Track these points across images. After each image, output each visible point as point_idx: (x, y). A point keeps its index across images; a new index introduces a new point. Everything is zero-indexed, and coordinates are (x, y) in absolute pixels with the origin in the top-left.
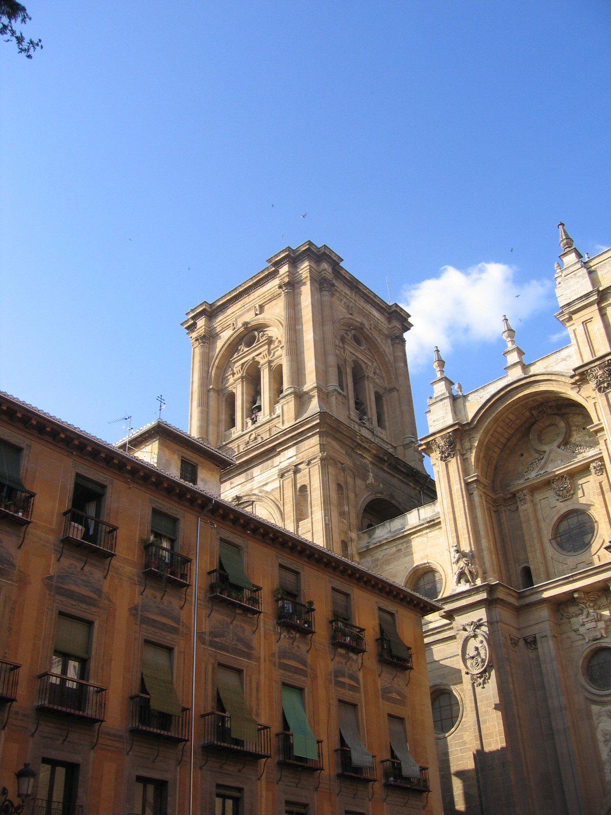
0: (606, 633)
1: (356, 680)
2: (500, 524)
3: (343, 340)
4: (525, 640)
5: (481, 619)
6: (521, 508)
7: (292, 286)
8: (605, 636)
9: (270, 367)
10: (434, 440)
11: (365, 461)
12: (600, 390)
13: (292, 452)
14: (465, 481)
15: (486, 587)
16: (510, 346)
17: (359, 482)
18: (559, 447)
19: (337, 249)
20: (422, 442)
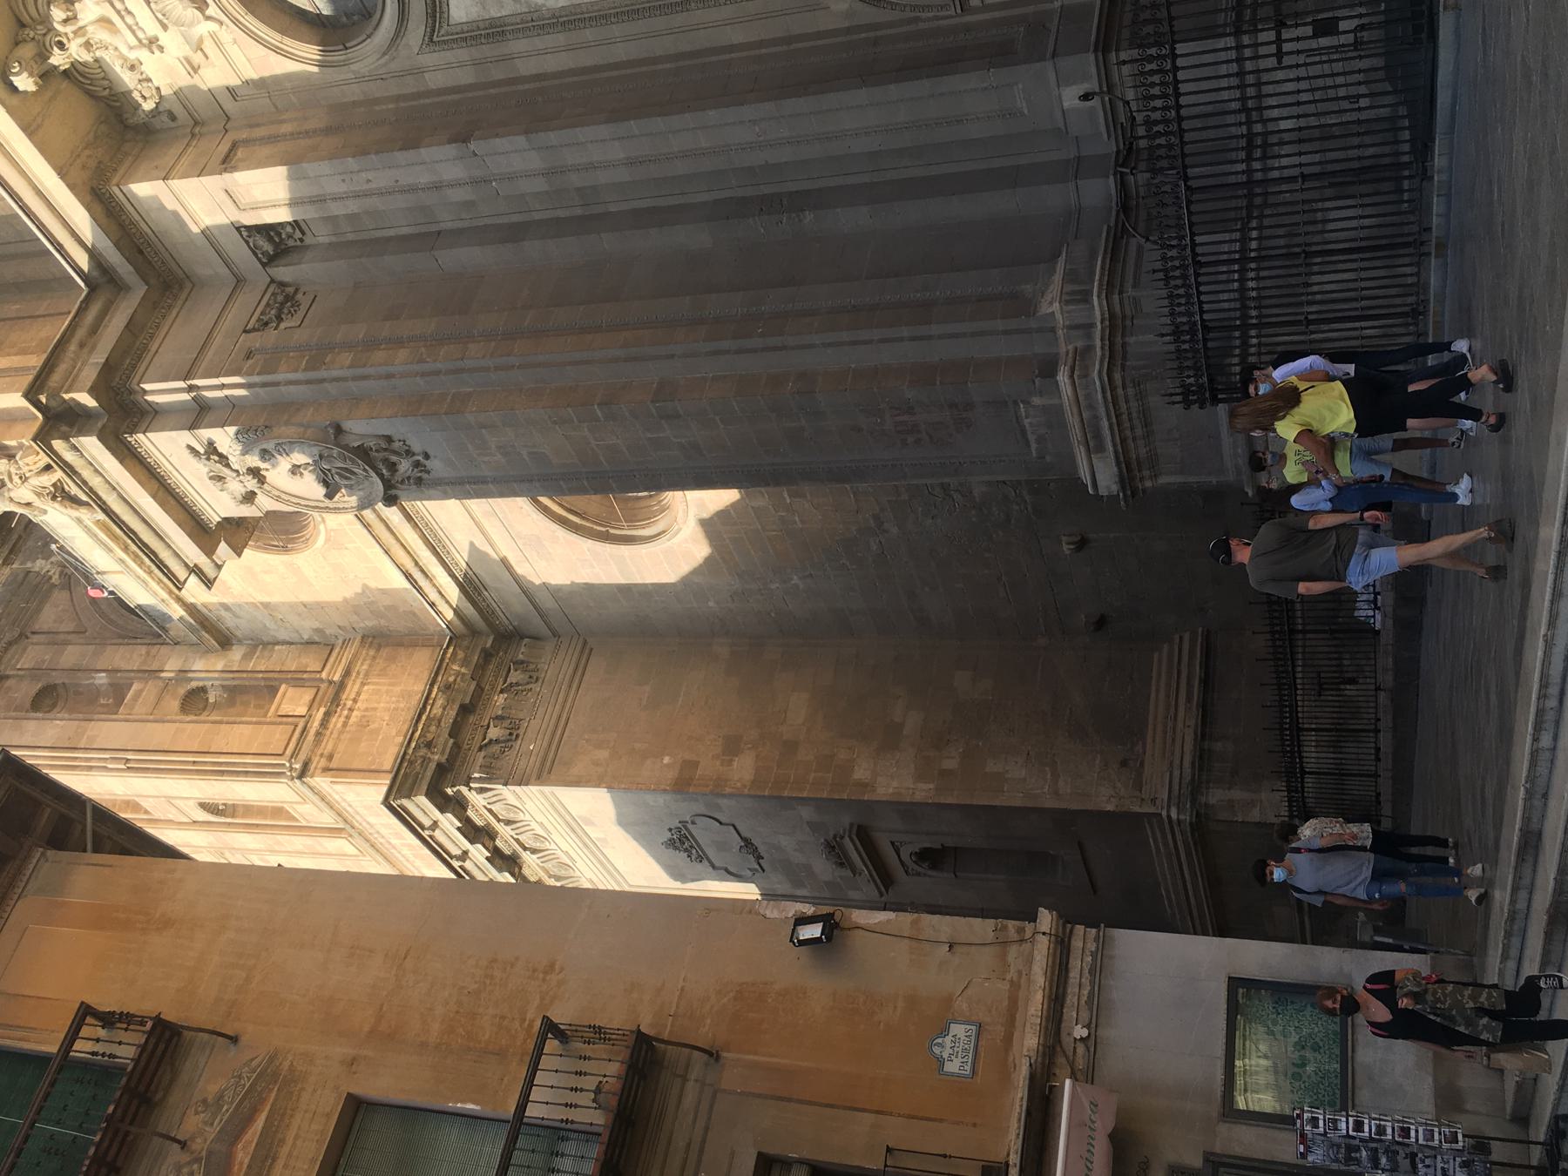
4: (269, 261)
5: (190, 448)
15: (58, 444)
17: (50, 616)
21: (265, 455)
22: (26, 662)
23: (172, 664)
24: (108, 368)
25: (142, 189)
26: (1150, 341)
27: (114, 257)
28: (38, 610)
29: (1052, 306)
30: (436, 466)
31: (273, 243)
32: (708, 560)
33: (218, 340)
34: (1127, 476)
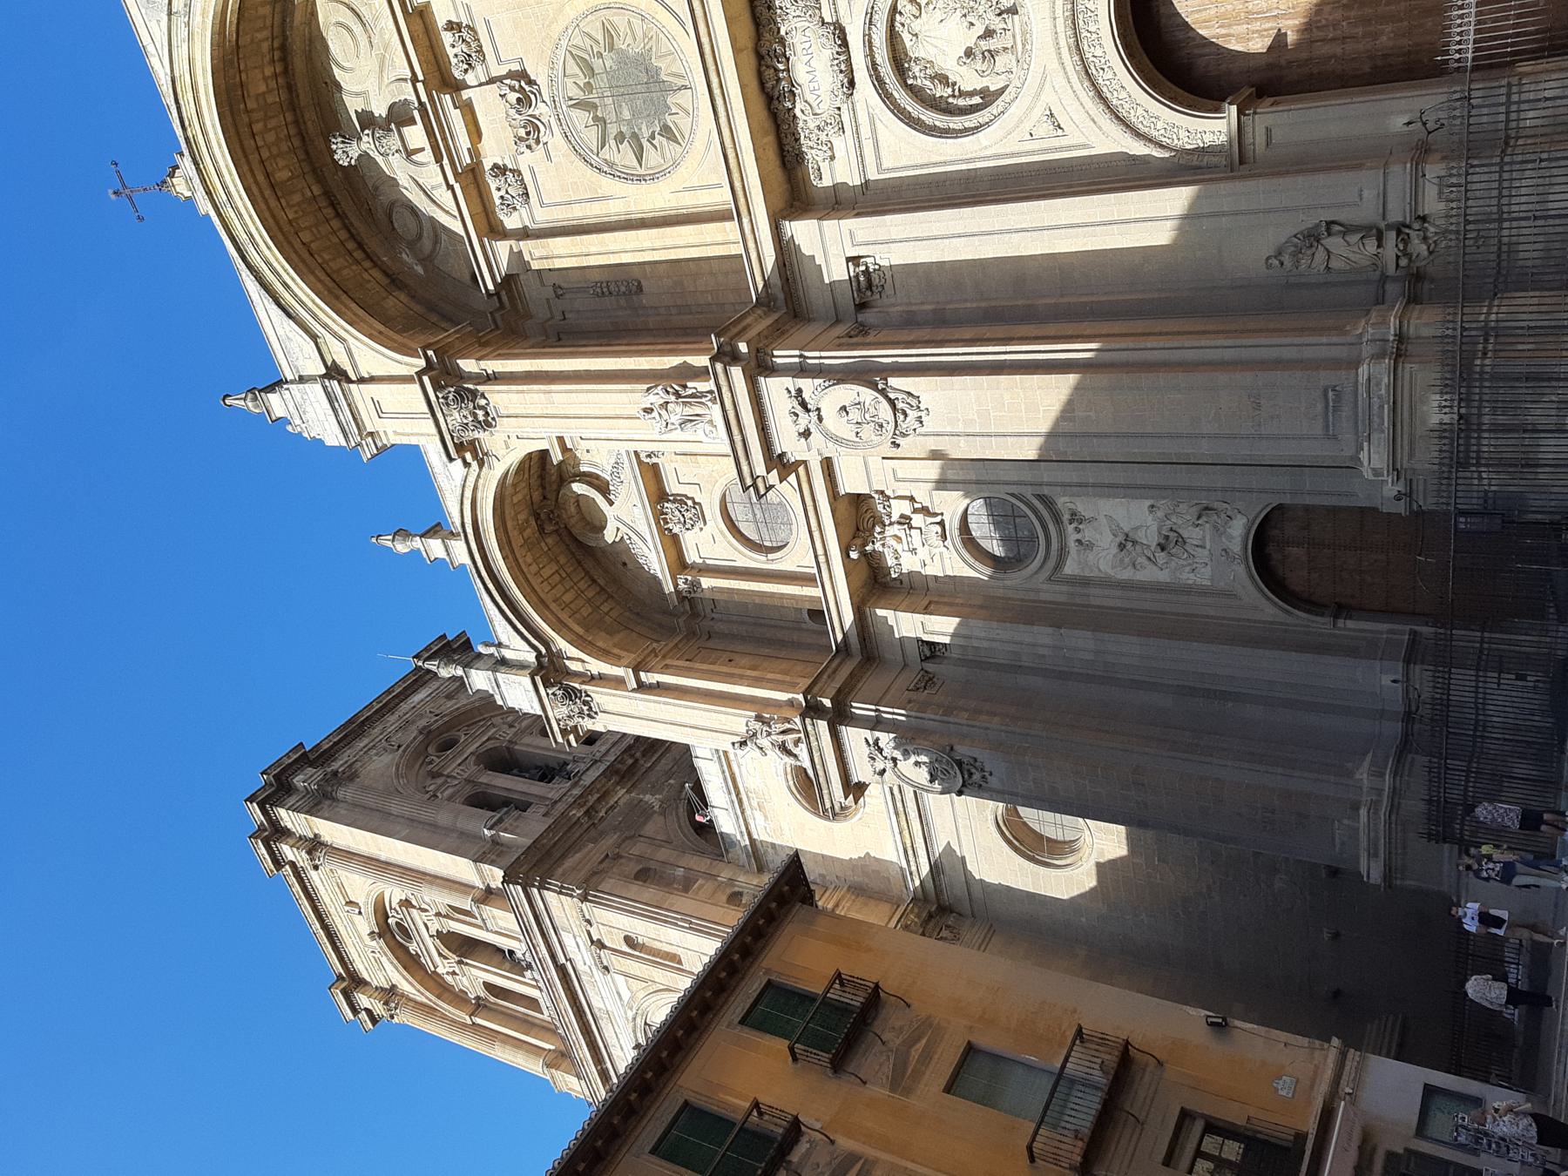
0: (936, 515)
1: (852, 1158)
2: (732, 637)
3: (434, 775)
6: (707, 595)
7: (314, 845)
8: (938, 519)
9: (447, 916)
10: (558, 721)
11: (621, 803)
12: (490, 425)
13: (567, 939)
14: (633, 690)
15: (808, 721)
16: (417, 543)
17: (649, 829)
18: (611, 503)
19: (278, 749)
20: (560, 740)
21: (906, 754)
22: (636, 850)
23: (725, 874)
24: (839, 691)
25: (880, 612)
26: (1415, 805)
27: (854, 640)
28: (645, 823)
29: (1363, 775)
30: (993, 782)
31: (931, 650)
32: (1093, 890)
33: (892, 691)
34: (1388, 875)
